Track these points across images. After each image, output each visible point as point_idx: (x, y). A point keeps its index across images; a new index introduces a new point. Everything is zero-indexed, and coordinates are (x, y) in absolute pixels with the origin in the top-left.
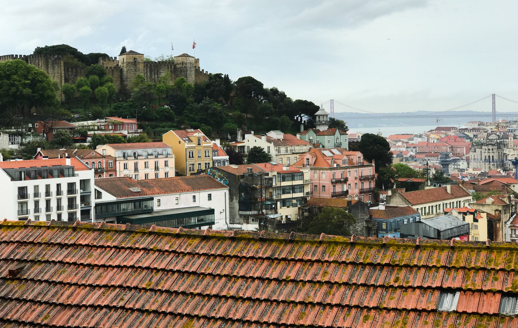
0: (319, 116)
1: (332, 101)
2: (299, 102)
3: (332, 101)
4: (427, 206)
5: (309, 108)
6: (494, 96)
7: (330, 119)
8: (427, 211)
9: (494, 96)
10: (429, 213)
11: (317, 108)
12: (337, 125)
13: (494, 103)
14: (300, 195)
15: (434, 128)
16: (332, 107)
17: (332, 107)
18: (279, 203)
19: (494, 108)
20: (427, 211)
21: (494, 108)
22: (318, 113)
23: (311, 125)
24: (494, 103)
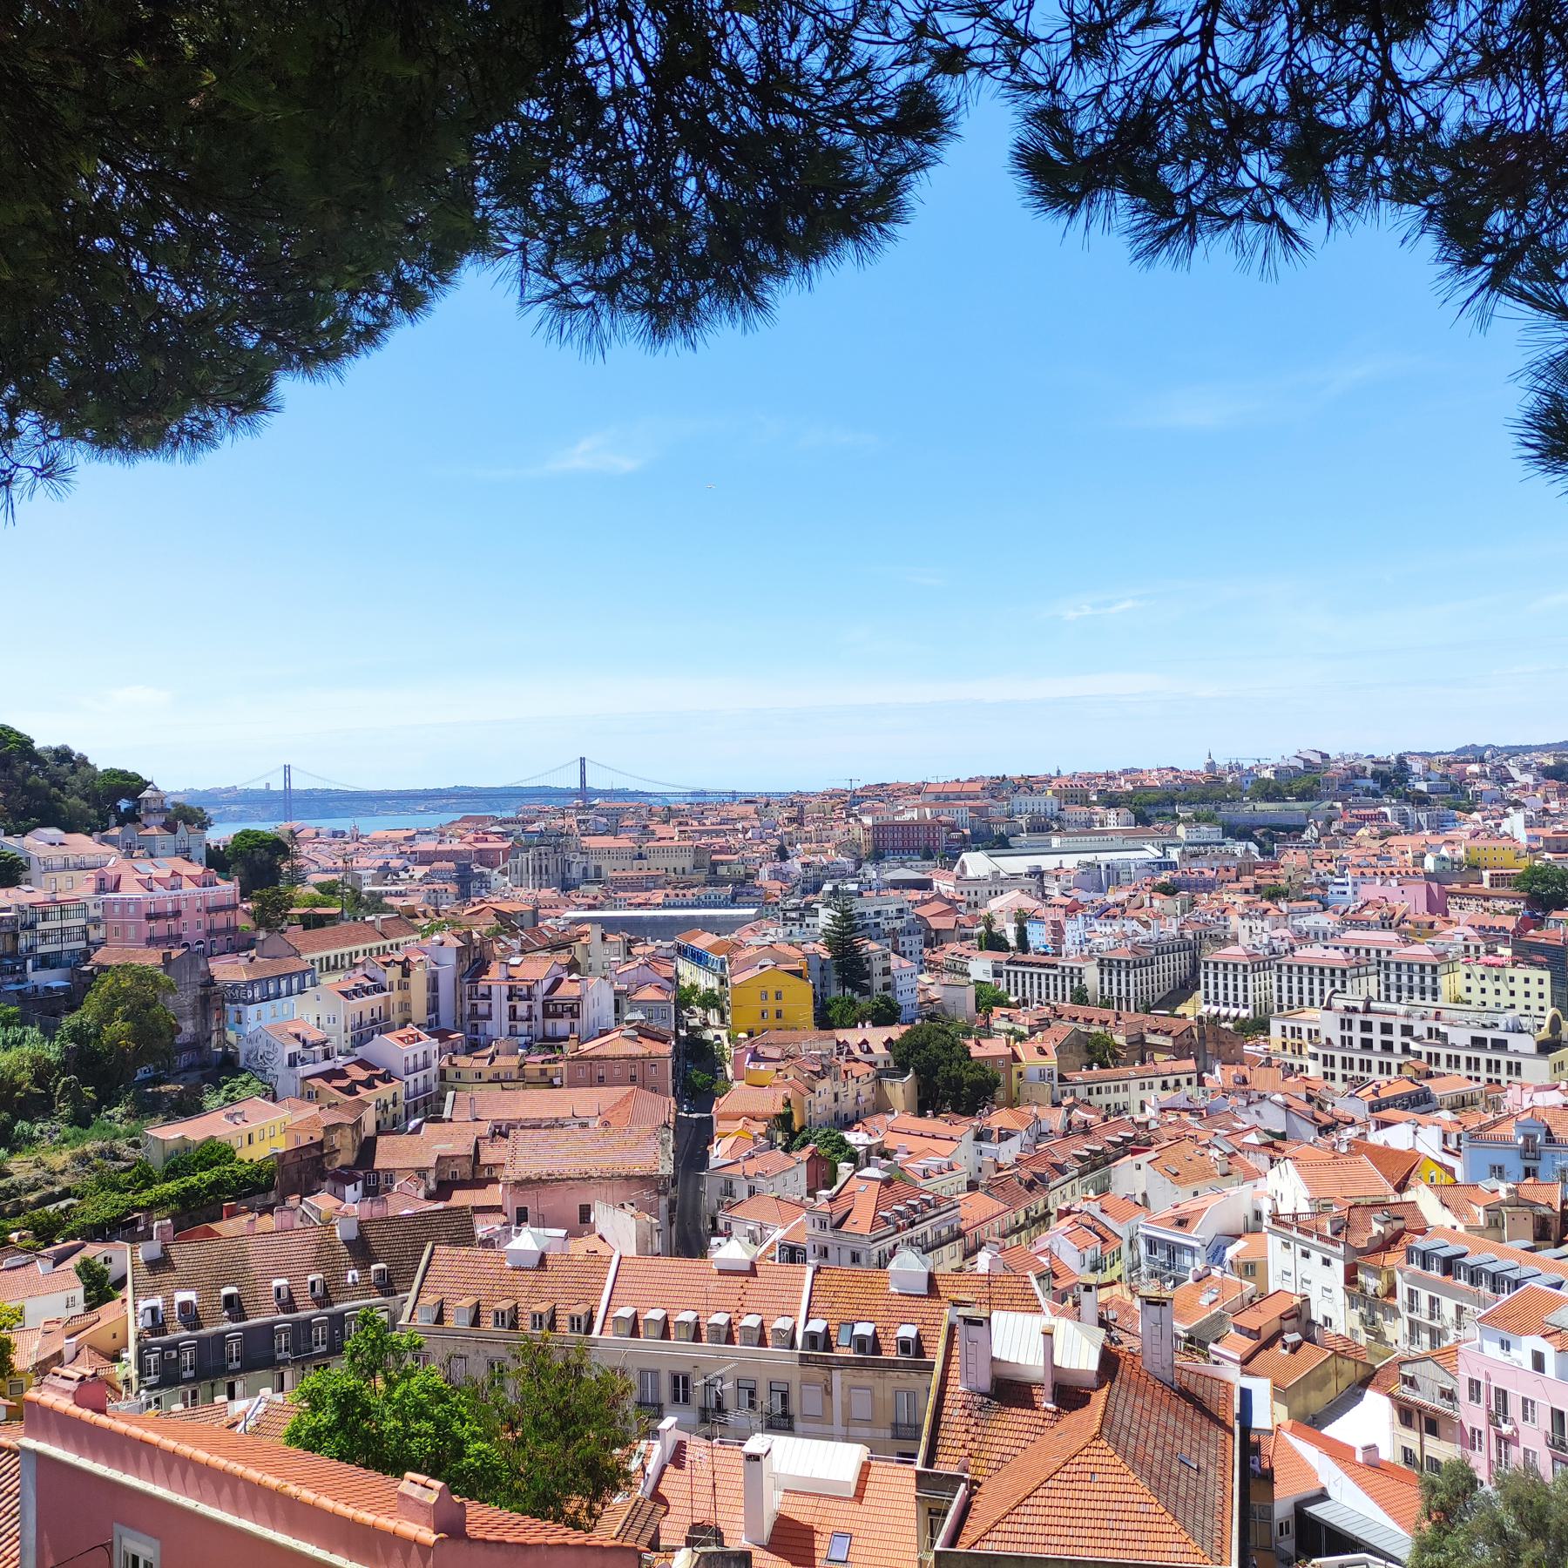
0: (147, 800)
1: (287, 769)
2: (112, 774)
3: (287, 769)
4: (331, 953)
5: (128, 785)
6: (583, 760)
7: (174, 804)
8: (332, 962)
9: (583, 760)
10: (335, 967)
11: (146, 785)
12: (186, 816)
13: (583, 773)
14: (83, 944)
15: (458, 817)
16: (287, 780)
17: (287, 780)
18: (30, 963)
19: (583, 781)
20: (332, 962)
21: (583, 781)
22: (146, 794)
23: (130, 818)
24: (583, 773)
